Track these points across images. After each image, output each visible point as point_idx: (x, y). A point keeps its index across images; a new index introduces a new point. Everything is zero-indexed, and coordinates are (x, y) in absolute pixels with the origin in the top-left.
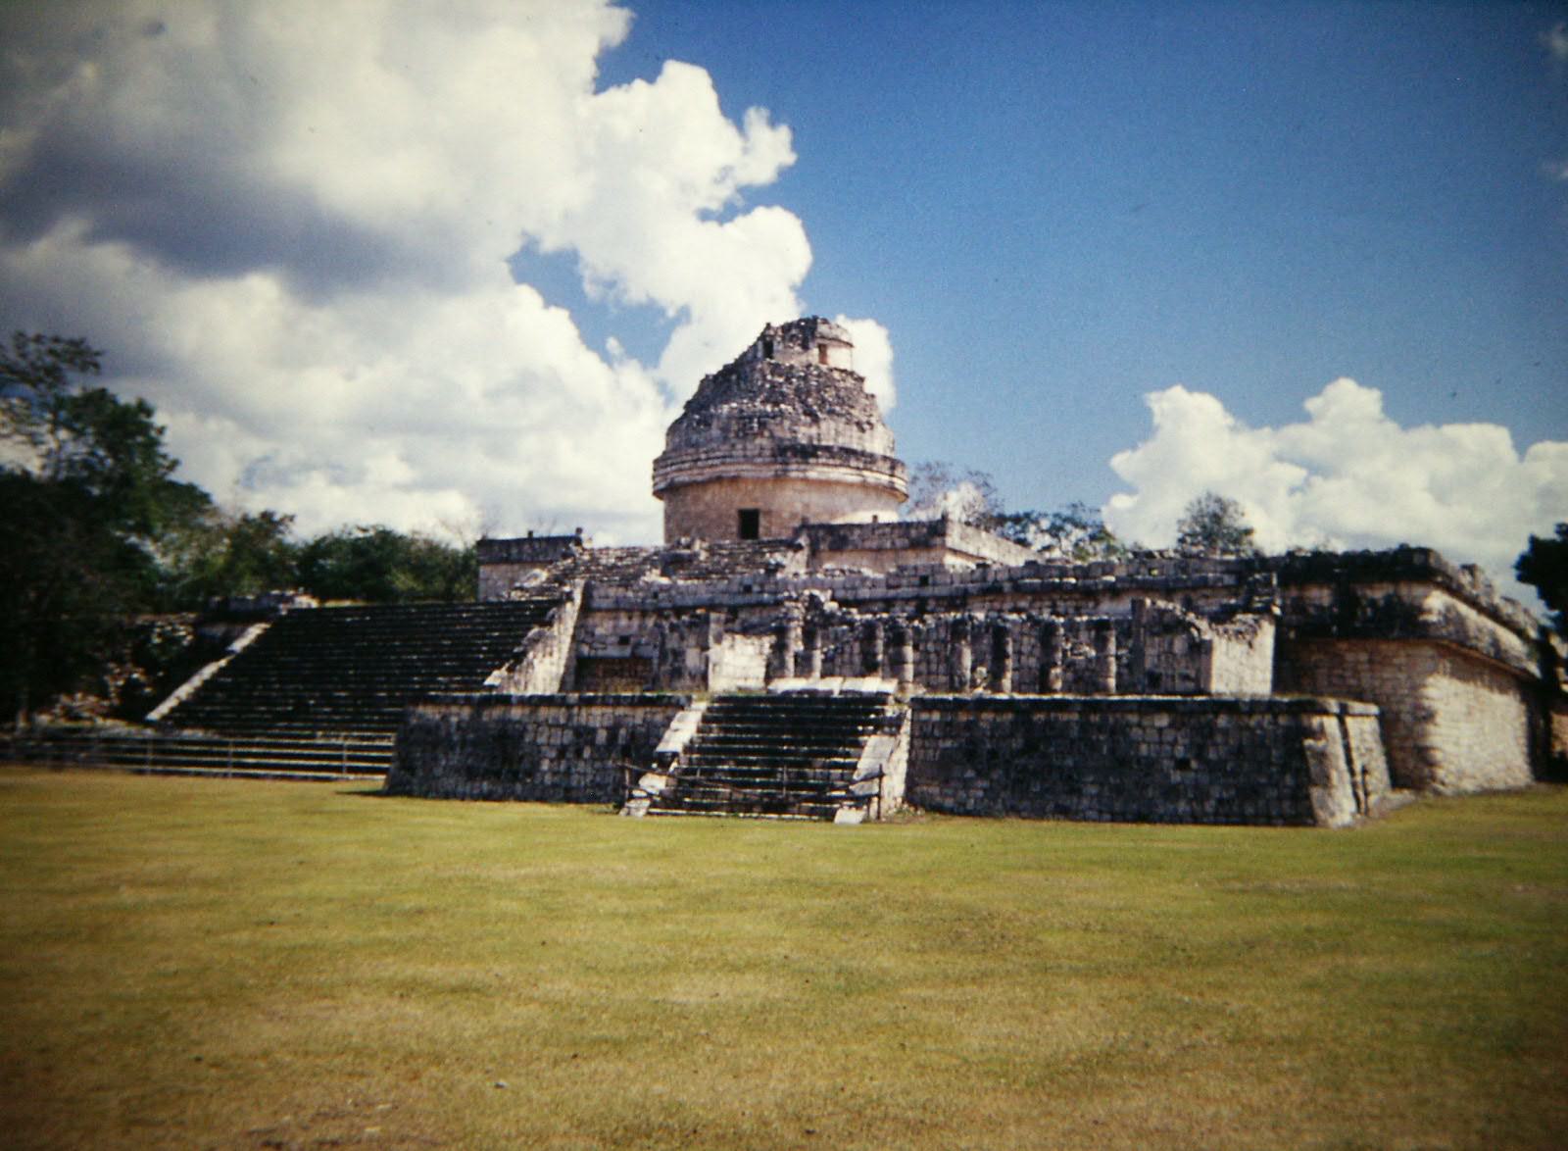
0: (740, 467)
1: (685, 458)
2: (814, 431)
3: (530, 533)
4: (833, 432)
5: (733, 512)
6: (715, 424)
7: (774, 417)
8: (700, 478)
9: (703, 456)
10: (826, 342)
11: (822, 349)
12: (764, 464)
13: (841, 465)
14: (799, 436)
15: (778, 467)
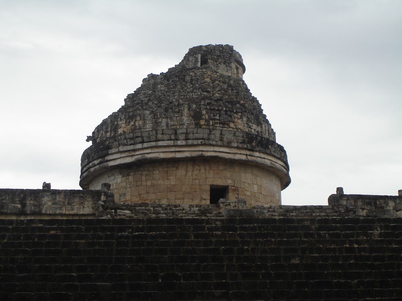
0: (217, 149)
1: (160, 136)
2: (259, 129)
3: (47, 186)
4: (267, 132)
5: (208, 188)
6: (186, 112)
7: (237, 113)
8: (178, 155)
9: (182, 137)
10: (239, 66)
11: (237, 68)
12: (238, 148)
13: (279, 159)
14: (253, 130)
15: (248, 153)
